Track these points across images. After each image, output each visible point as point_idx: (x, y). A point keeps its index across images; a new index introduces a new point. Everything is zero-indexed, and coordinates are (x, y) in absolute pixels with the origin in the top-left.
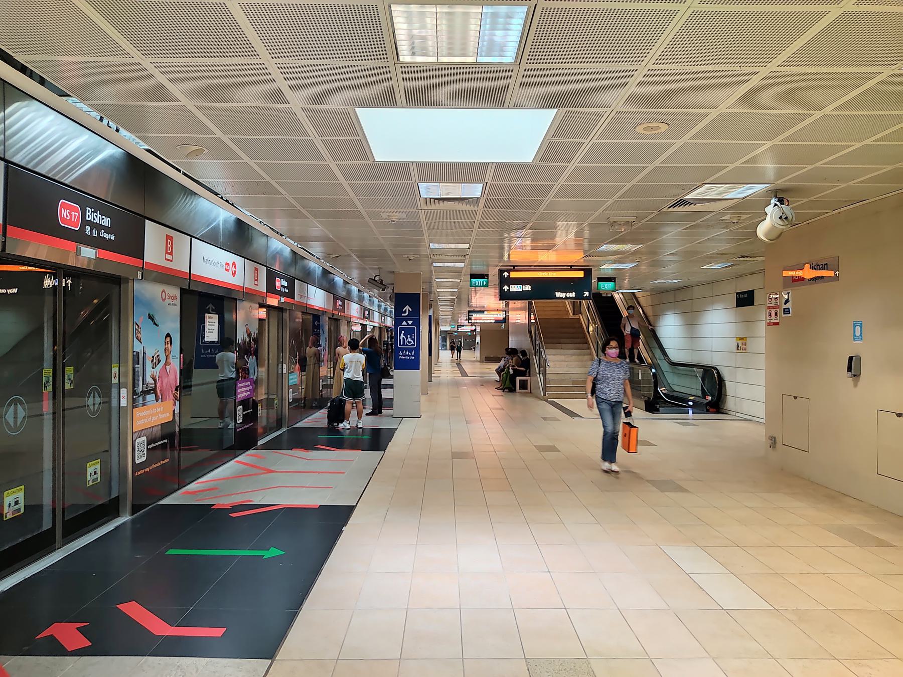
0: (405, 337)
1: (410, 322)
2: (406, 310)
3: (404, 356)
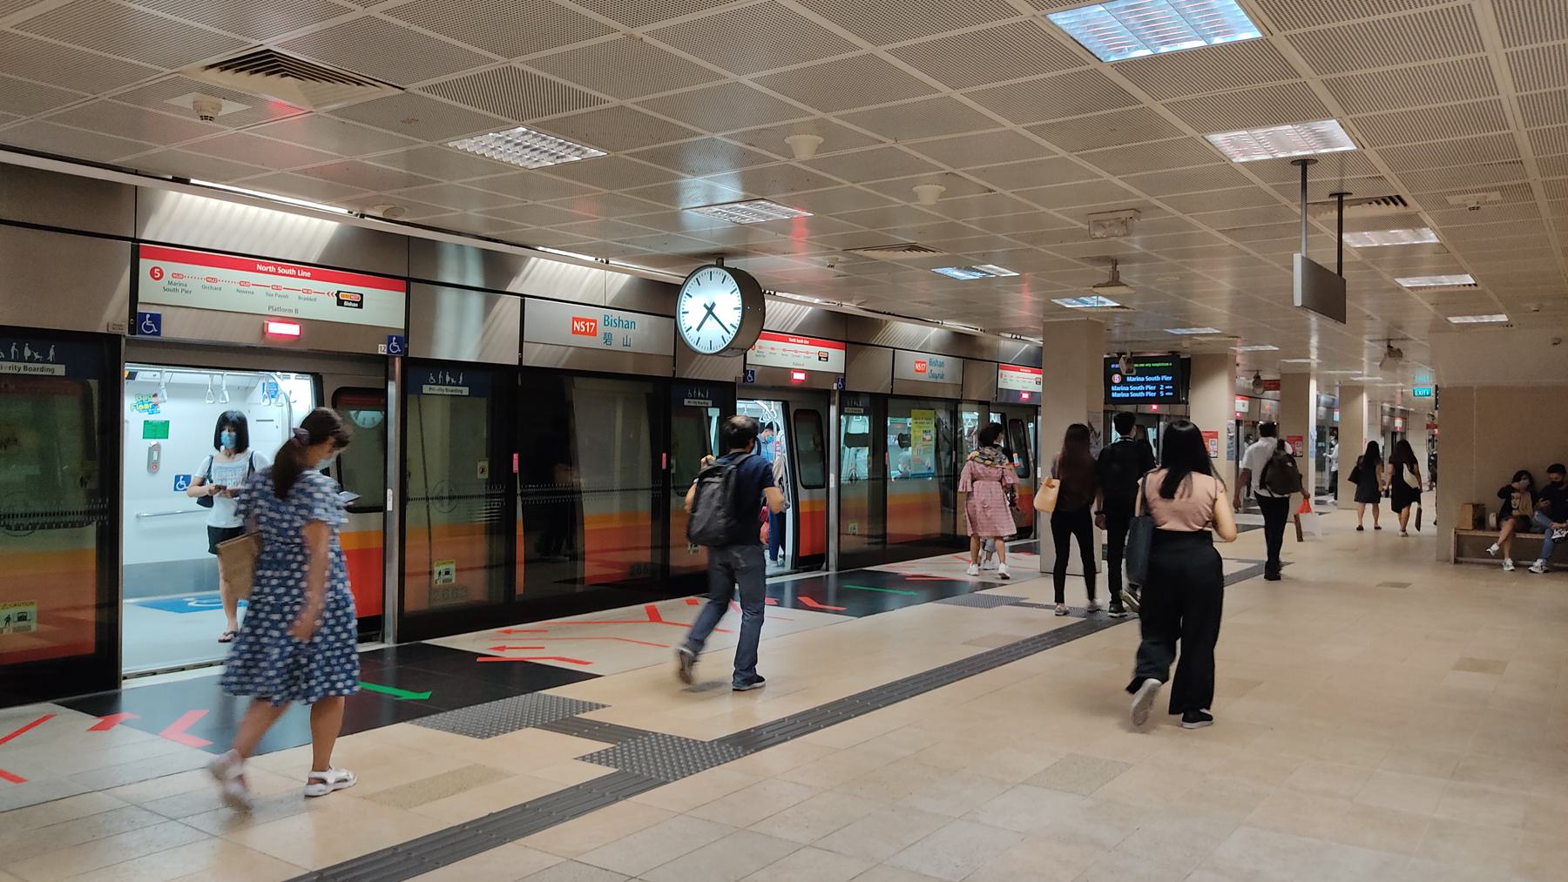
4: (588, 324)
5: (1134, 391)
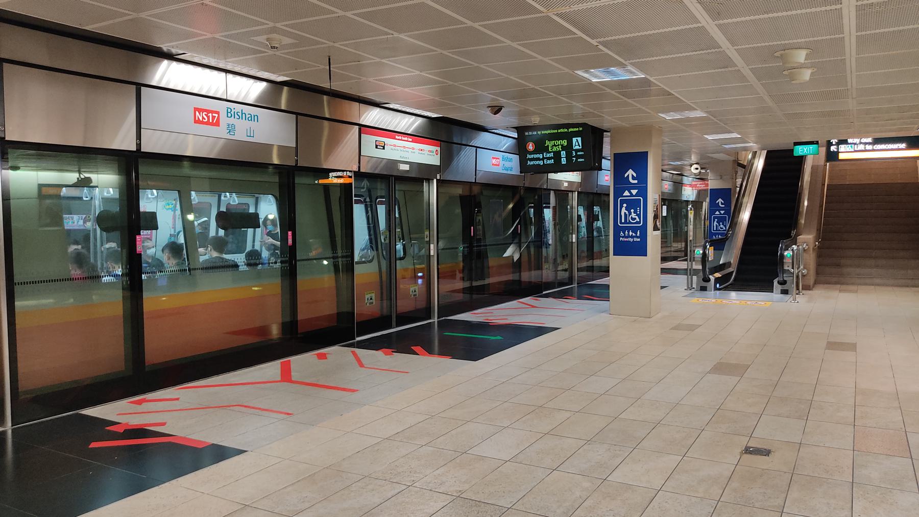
0: (627, 212)
1: (634, 192)
2: (628, 175)
3: (627, 237)
4: (210, 115)
5: (538, 159)
